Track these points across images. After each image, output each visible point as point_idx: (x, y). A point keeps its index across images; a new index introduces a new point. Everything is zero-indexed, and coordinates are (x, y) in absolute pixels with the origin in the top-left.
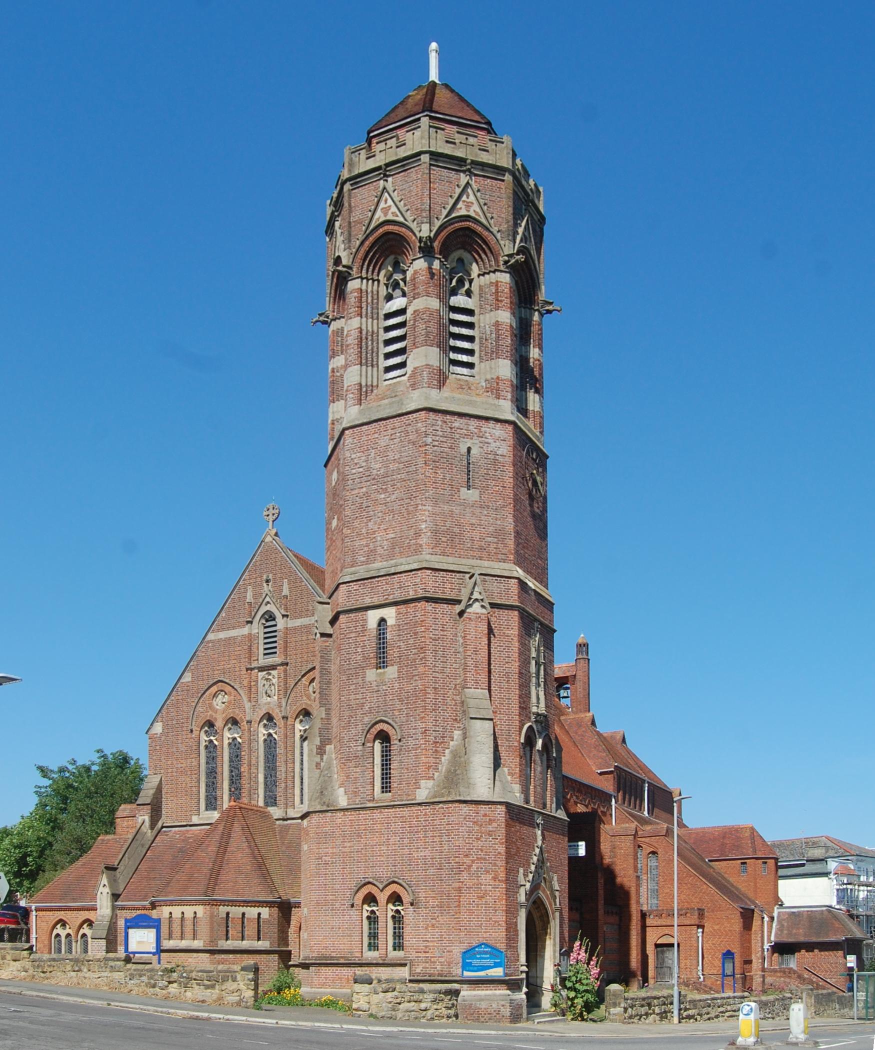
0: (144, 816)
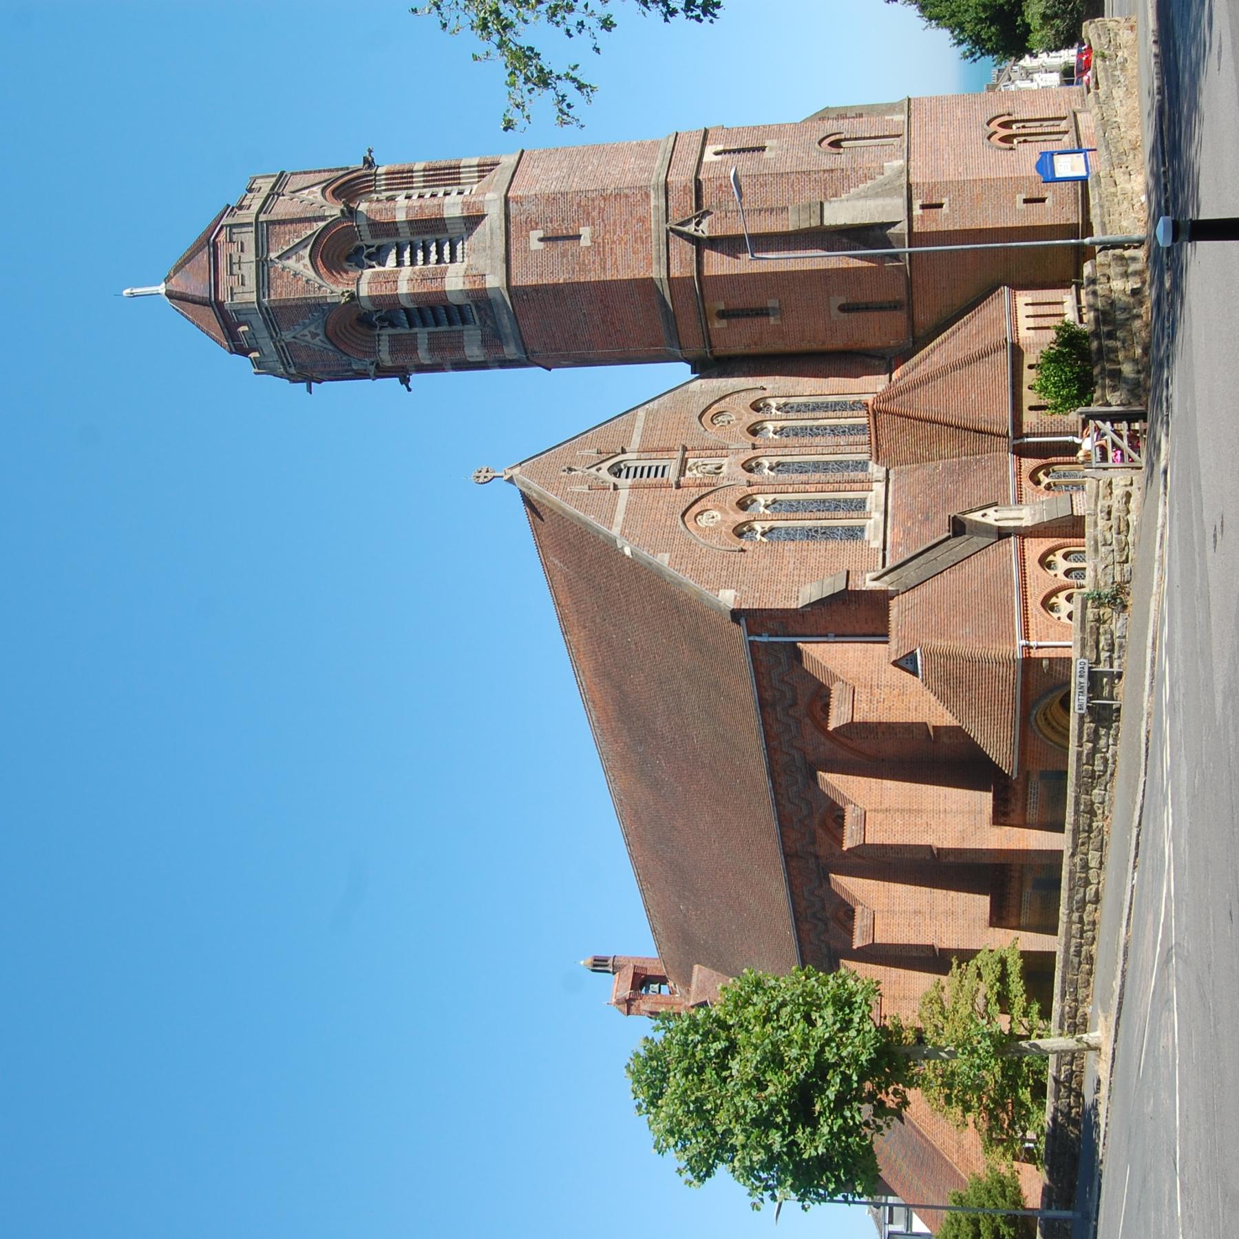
0: (865, 579)
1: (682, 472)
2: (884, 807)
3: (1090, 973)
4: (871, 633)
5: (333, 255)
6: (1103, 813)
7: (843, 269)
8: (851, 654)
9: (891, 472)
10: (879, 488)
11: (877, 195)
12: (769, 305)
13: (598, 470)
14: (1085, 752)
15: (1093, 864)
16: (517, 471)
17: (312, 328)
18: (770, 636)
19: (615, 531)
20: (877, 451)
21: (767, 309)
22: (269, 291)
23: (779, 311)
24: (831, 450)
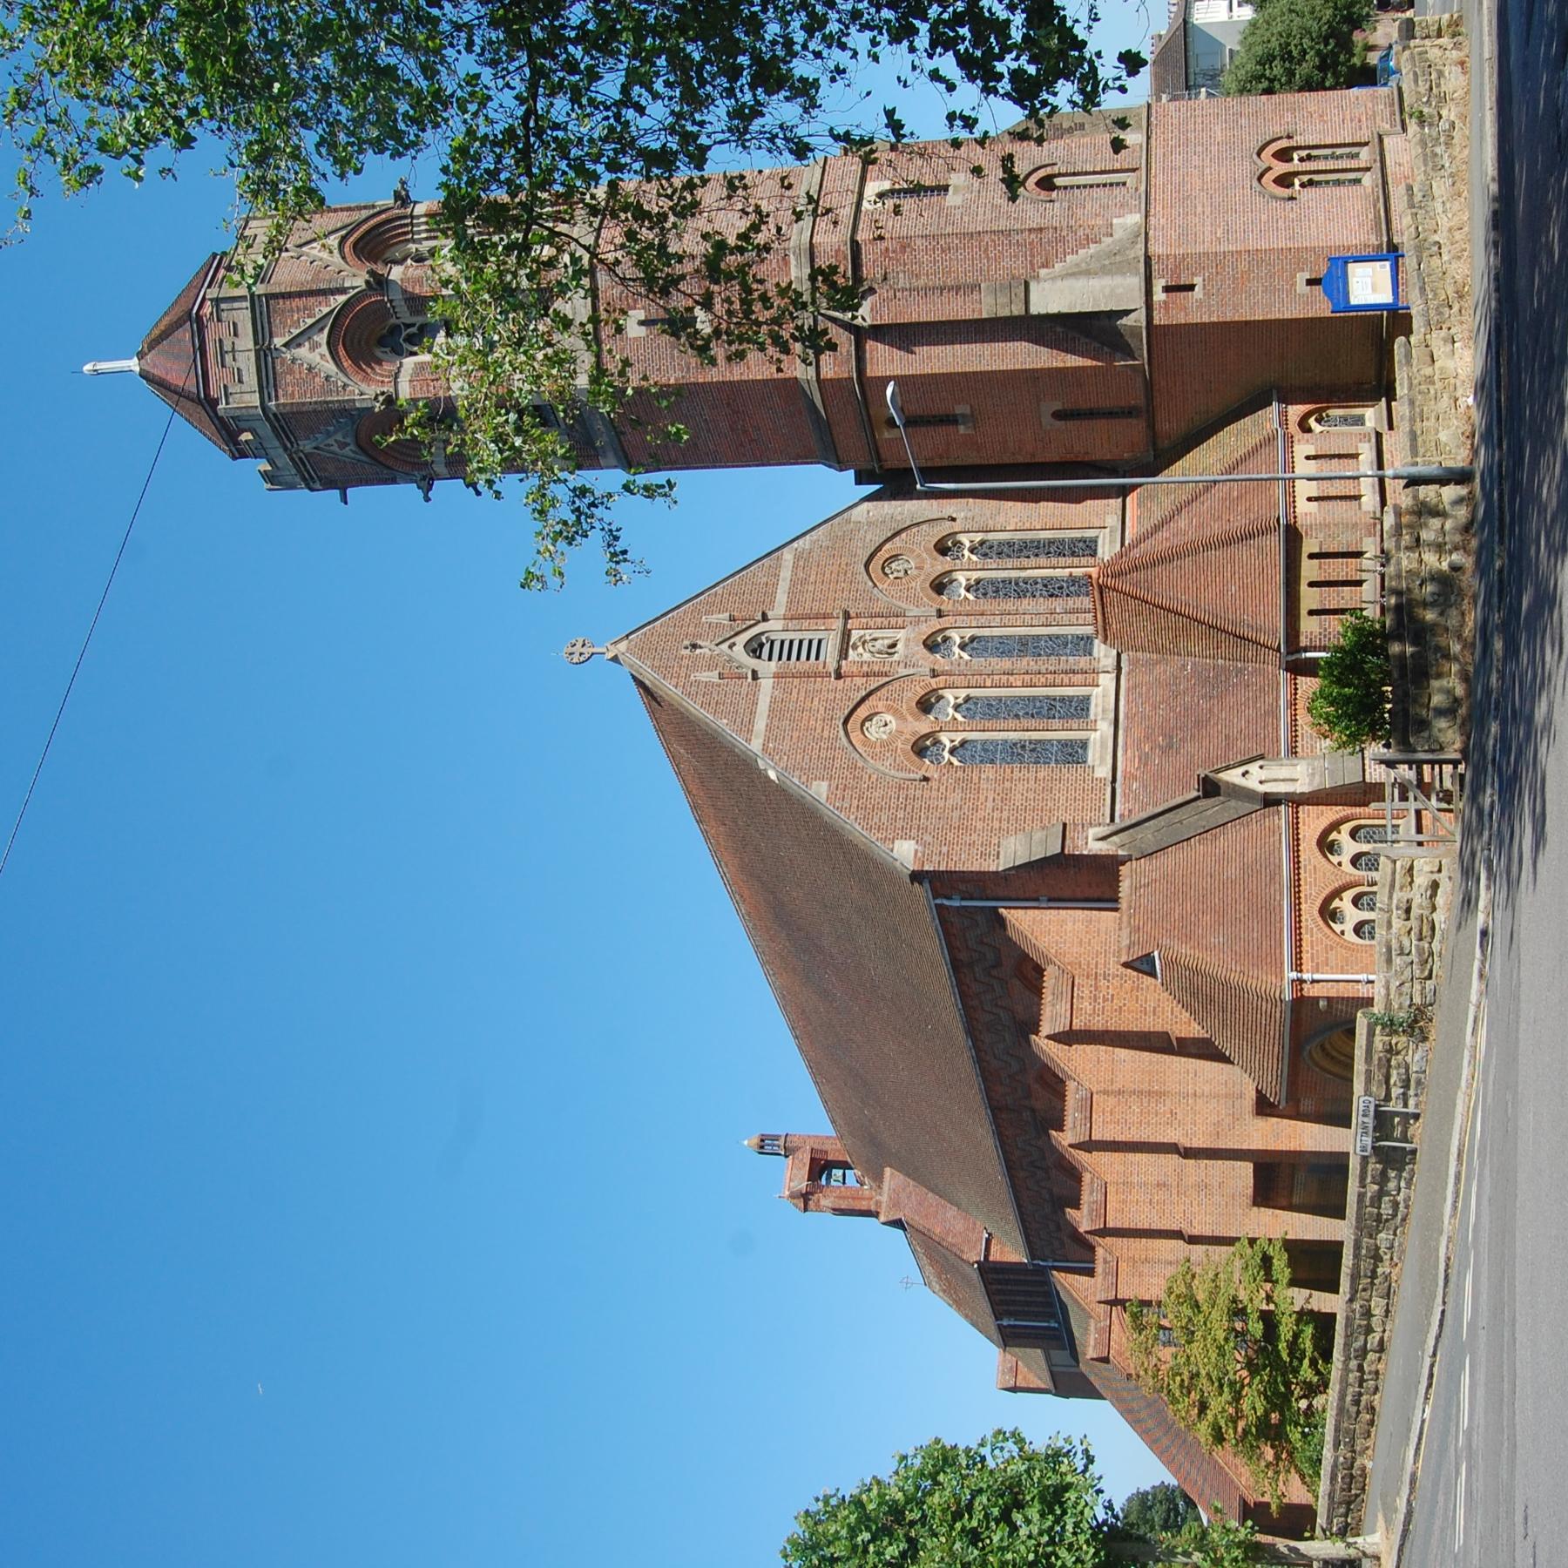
1: (843, 654)
2: (1116, 1087)
3: (1372, 1423)
4: (1096, 896)
5: (359, 342)
6: (1392, 1259)
7: (1058, 370)
8: (1069, 926)
9: (1124, 657)
10: (1107, 681)
11: (1104, 271)
12: (957, 412)
13: (731, 647)
14: (1369, 1195)
15: (1378, 1311)
16: (623, 646)
17: (339, 437)
18: (963, 899)
19: (756, 745)
20: (1105, 630)
21: (955, 416)
22: (276, 391)
23: (971, 419)
24: (1043, 619)
